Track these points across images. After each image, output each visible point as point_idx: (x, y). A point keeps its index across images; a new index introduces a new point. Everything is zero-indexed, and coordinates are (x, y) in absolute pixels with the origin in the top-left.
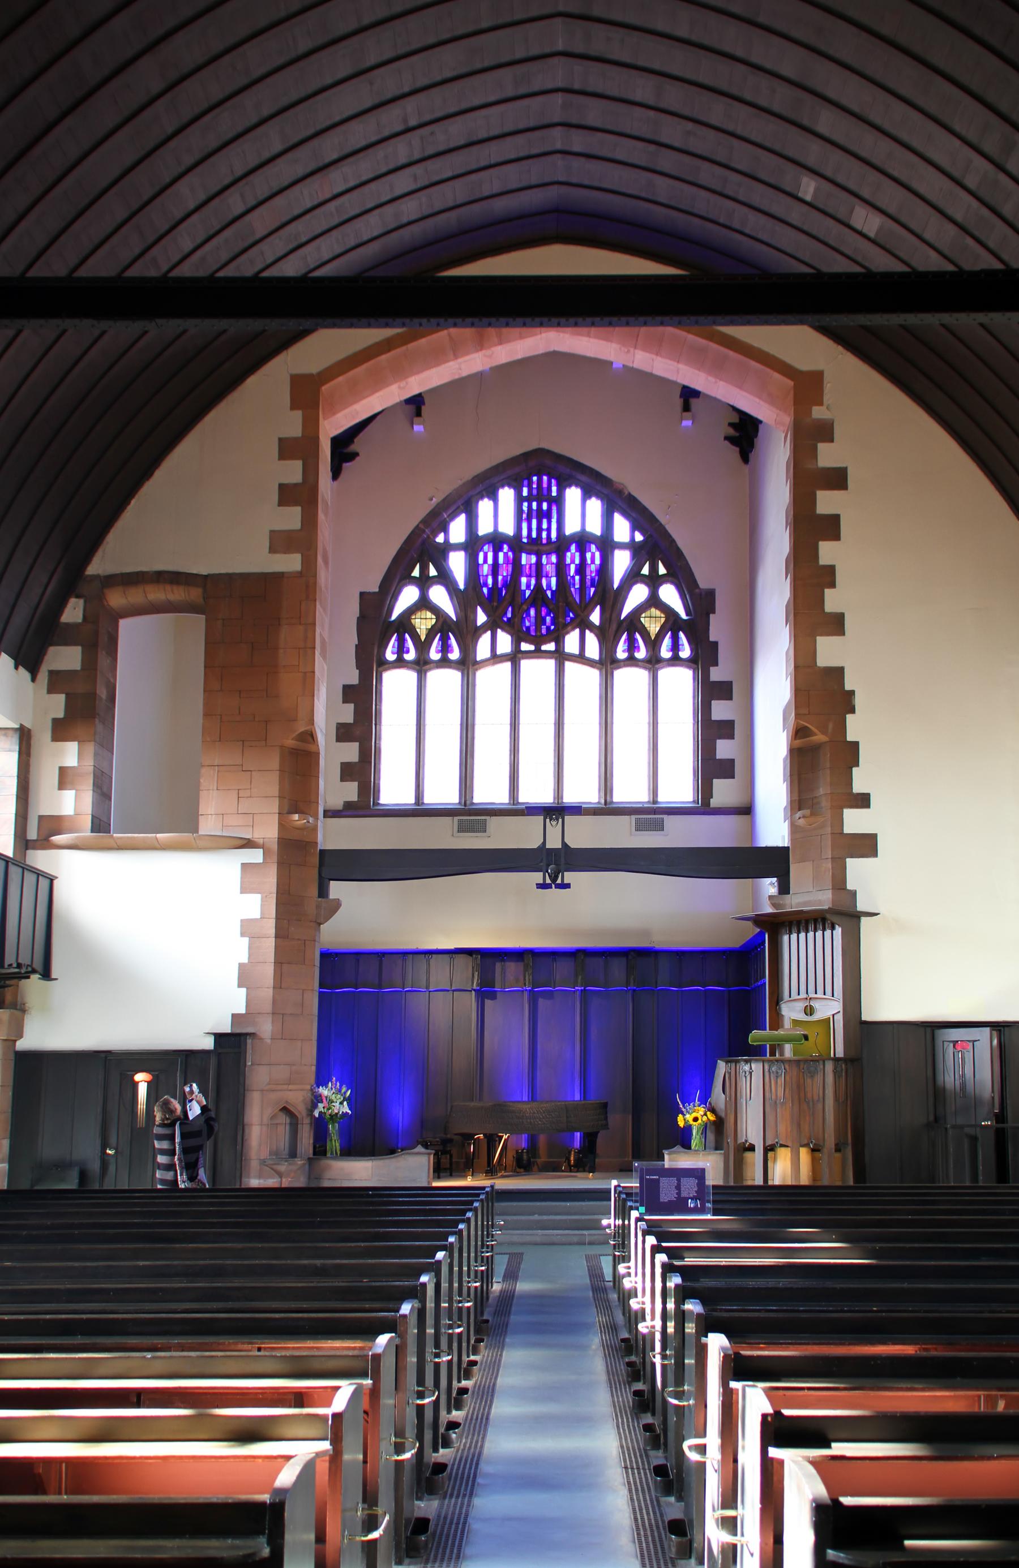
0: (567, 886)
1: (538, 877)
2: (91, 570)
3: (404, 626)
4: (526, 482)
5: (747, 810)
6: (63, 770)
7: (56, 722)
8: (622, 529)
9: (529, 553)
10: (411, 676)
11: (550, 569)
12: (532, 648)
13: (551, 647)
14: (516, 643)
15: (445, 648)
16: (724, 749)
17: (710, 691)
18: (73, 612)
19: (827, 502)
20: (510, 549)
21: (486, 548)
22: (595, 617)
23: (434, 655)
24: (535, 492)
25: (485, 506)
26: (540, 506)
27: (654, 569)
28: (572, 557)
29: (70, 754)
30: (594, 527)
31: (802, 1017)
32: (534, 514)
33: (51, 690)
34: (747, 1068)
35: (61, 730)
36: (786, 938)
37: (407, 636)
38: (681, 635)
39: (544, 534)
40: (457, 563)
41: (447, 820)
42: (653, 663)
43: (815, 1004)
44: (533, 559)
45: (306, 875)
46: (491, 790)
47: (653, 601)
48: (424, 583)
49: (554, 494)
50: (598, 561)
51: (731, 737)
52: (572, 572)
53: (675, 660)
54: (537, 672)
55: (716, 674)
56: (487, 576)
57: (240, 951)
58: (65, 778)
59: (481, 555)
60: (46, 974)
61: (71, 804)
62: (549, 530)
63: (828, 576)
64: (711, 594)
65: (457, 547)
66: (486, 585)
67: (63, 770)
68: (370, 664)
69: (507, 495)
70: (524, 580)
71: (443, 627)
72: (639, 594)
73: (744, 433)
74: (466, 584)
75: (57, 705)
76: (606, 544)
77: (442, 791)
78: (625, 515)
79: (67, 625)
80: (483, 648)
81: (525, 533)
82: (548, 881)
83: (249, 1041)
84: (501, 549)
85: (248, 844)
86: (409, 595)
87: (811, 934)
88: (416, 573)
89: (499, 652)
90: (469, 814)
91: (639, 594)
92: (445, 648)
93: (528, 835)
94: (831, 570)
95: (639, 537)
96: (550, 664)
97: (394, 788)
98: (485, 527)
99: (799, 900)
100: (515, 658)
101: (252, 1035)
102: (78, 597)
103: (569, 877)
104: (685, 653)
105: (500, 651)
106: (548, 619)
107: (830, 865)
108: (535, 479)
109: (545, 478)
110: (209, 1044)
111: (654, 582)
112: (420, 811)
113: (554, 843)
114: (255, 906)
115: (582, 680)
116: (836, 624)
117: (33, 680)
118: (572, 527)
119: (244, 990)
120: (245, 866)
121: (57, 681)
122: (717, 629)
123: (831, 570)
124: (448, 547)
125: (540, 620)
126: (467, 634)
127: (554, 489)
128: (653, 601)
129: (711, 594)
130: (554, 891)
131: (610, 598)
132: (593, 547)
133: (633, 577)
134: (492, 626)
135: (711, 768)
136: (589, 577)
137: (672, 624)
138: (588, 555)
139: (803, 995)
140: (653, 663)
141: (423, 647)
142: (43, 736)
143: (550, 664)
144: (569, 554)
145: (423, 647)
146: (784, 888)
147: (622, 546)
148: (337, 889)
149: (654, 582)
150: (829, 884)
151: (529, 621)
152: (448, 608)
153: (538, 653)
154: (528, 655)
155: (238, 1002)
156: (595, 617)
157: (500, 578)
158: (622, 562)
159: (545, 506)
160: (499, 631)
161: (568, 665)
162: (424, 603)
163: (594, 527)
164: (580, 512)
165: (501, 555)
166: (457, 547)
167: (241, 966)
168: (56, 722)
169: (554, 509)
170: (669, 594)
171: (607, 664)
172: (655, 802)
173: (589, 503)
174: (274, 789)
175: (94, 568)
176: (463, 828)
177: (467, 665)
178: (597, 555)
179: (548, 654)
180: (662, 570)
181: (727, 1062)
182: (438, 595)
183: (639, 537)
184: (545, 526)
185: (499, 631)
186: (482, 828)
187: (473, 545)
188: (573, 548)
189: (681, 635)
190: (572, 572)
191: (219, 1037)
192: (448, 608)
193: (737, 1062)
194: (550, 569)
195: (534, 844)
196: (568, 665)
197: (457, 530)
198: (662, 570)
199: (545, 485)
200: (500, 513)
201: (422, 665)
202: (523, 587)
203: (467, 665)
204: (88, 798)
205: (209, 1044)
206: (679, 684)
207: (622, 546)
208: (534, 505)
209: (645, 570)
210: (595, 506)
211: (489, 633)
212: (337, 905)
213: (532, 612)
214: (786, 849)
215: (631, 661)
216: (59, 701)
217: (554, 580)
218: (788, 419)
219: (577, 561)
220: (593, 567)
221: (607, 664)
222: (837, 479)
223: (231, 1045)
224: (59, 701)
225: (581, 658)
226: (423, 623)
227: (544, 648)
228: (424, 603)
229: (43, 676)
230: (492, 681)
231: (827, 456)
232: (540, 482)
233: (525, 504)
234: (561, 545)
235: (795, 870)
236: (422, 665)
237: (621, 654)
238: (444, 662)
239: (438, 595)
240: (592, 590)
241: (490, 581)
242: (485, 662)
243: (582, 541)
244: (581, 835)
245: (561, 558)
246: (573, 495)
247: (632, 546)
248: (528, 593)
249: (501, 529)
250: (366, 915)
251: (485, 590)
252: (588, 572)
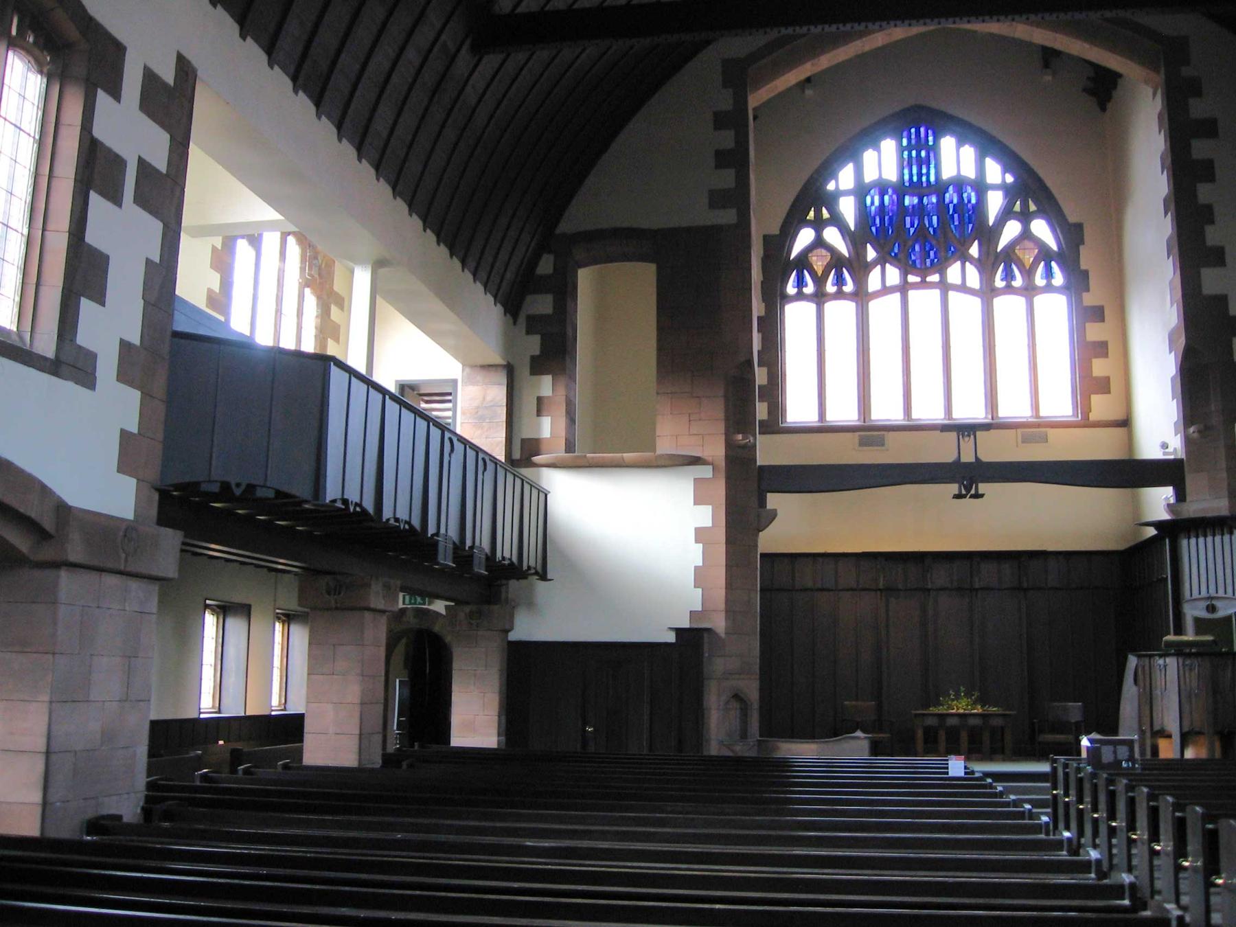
0: (977, 496)
1: (954, 488)
2: (558, 231)
3: (803, 263)
4: (905, 134)
5: (1126, 423)
6: (540, 400)
7: (533, 358)
8: (994, 172)
9: (912, 195)
10: (809, 308)
12: (918, 279)
13: (935, 278)
14: (904, 275)
15: (840, 281)
16: (1100, 367)
17: (1086, 315)
18: (546, 266)
19: (1201, 149)
20: (895, 192)
22: (974, 250)
23: (830, 288)
24: (913, 142)
25: (869, 156)
27: (1025, 206)
28: (951, 196)
29: (545, 385)
30: (969, 172)
31: (1203, 614)
32: (914, 161)
33: (528, 333)
34: (1161, 661)
35: (539, 366)
36: (1184, 542)
37: (806, 272)
38: (1053, 264)
39: (924, 179)
40: (848, 208)
41: (849, 435)
42: (1029, 291)
43: (1217, 603)
44: (916, 200)
45: (748, 488)
46: (887, 409)
47: (1026, 234)
48: (819, 225)
49: (931, 143)
50: (973, 201)
51: (1106, 355)
53: (1049, 288)
54: (924, 301)
55: (1089, 299)
57: (695, 555)
58: (541, 406)
60: (543, 577)
61: (548, 428)
62: (928, 174)
63: (1206, 215)
64: (1079, 227)
65: (847, 193)
66: (874, 224)
67: (540, 400)
68: (775, 299)
69: (889, 146)
70: (908, 219)
71: (837, 263)
72: (1013, 229)
73: (1102, 87)
74: (856, 226)
75: (533, 345)
76: (981, 187)
77: (843, 411)
78: (997, 159)
79: (541, 277)
80: (874, 281)
81: (906, 177)
82: (964, 492)
83: (706, 635)
84: (887, 193)
85: (695, 461)
86: (805, 237)
87: (1209, 539)
88: (812, 214)
89: (888, 284)
90: (869, 432)
91: (1013, 229)
92: (840, 281)
93: (944, 451)
94: (1209, 208)
95: (1010, 179)
96: (936, 293)
97: (799, 407)
98: (870, 176)
99: (1196, 507)
100: (903, 288)
101: (708, 630)
102: (549, 252)
103: (983, 487)
104: (1058, 279)
105: (888, 284)
106: (932, 253)
107: (1225, 475)
108: (913, 130)
109: (922, 130)
110: (671, 638)
111: (1025, 218)
112: (824, 429)
113: (968, 457)
114: (704, 516)
115: (966, 309)
116: (1217, 257)
117: (515, 323)
118: (948, 172)
119: (700, 590)
120: (697, 481)
121: (534, 324)
122: (1087, 258)
123: (1209, 208)
124: (837, 194)
126: (860, 268)
127: (931, 138)
128: (1026, 234)
129: (1079, 227)
130: (967, 500)
131: (988, 235)
132: (969, 189)
133: (1007, 214)
134: (881, 261)
135: (1088, 385)
137: (1045, 255)
138: (965, 195)
139: (1204, 593)
140: (1029, 291)
141: (820, 281)
142: (523, 371)
143: (936, 293)
144: (947, 195)
145: (820, 281)
146: (1181, 496)
147: (995, 187)
148: (774, 500)
149: (1025, 218)
150: (1225, 493)
152: (842, 247)
153: (924, 284)
154: (915, 286)
155: (695, 600)
156: (974, 250)
158: (995, 202)
159: (923, 154)
161: (951, 294)
162: (819, 243)
164: (955, 158)
165: (886, 198)
166: (847, 193)
167: (696, 568)
168: (533, 358)
169: (932, 155)
170: (1041, 229)
171: (987, 293)
172: (1037, 416)
173: (962, 149)
174: (722, 415)
175: (565, 227)
176: (863, 443)
177: (861, 297)
178: (973, 194)
179: (932, 285)
180: (1033, 207)
181: (1139, 656)
182: (832, 235)
183: (1010, 179)
184: (924, 171)
186: (880, 443)
187: (861, 191)
189: (1053, 264)
191: (679, 631)
192: (842, 247)
193: (1151, 656)
195: (950, 458)
196: (951, 294)
197: (845, 178)
198: (1033, 207)
199: (923, 135)
200: (883, 161)
201: (820, 297)
202: (908, 225)
203: (861, 297)
204: (562, 422)
205: (671, 638)
206: (1054, 310)
207: (995, 187)
208: (914, 153)
209: (1017, 207)
210: (968, 152)
211: (879, 267)
212: (773, 515)
213: (917, 248)
214: (1181, 461)
215: (1009, 289)
216: (535, 340)
217: (935, 218)
218: (1160, 78)
219: (955, 201)
221: (987, 293)
222: (1209, 128)
223: (691, 639)
224: (535, 340)
225: (963, 288)
226: (819, 261)
227: (929, 279)
228: (819, 243)
229: (522, 320)
230: (884, 311)
231: (1198, 109)
233: (906, 153)
234: (940, 188)
235: (1192, 482)
236: (820, 297)
237: (999, 283)
238: (840, 295)
239: (832, 235)
242: (877, 294)
243: (959, 184)
244: (994, 450)
245: (941, 198)
246: (948, 144)
247: (1004, 187)
248: (912, 230)
249: (884, 177)
250: (795, 525)
251: (874, 229)
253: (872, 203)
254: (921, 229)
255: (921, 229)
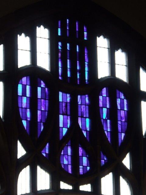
9: (65, 92)
11: (83, 109)
21: (24, 80)
25: (23, 42)
26: (73, 48)
52: (104, 116)
56: (26, 108)
59: (20, 87)
106: (85, 160)
125: (76, 161)
136: (120, 122)
138: (119, 101)
151: (67, 159)
156: (127, 162)
157: (39, 112)
160: (39, 168)
163: (122, 74)
164: (109, 61)
185: (39, 168)
188: (104, 91)
190: (104, 116)
194: (83, 109)
202: (61, 125)
210: (121, 57)
220: (122, 113)
232: (72, 25)
240: (123, 135)
241: (28, 114)
248: (65, 131)
251: (24, 123)
252: (119, 118)
253: (24, 94)
254: (74, 129)
255: (74, 129)
